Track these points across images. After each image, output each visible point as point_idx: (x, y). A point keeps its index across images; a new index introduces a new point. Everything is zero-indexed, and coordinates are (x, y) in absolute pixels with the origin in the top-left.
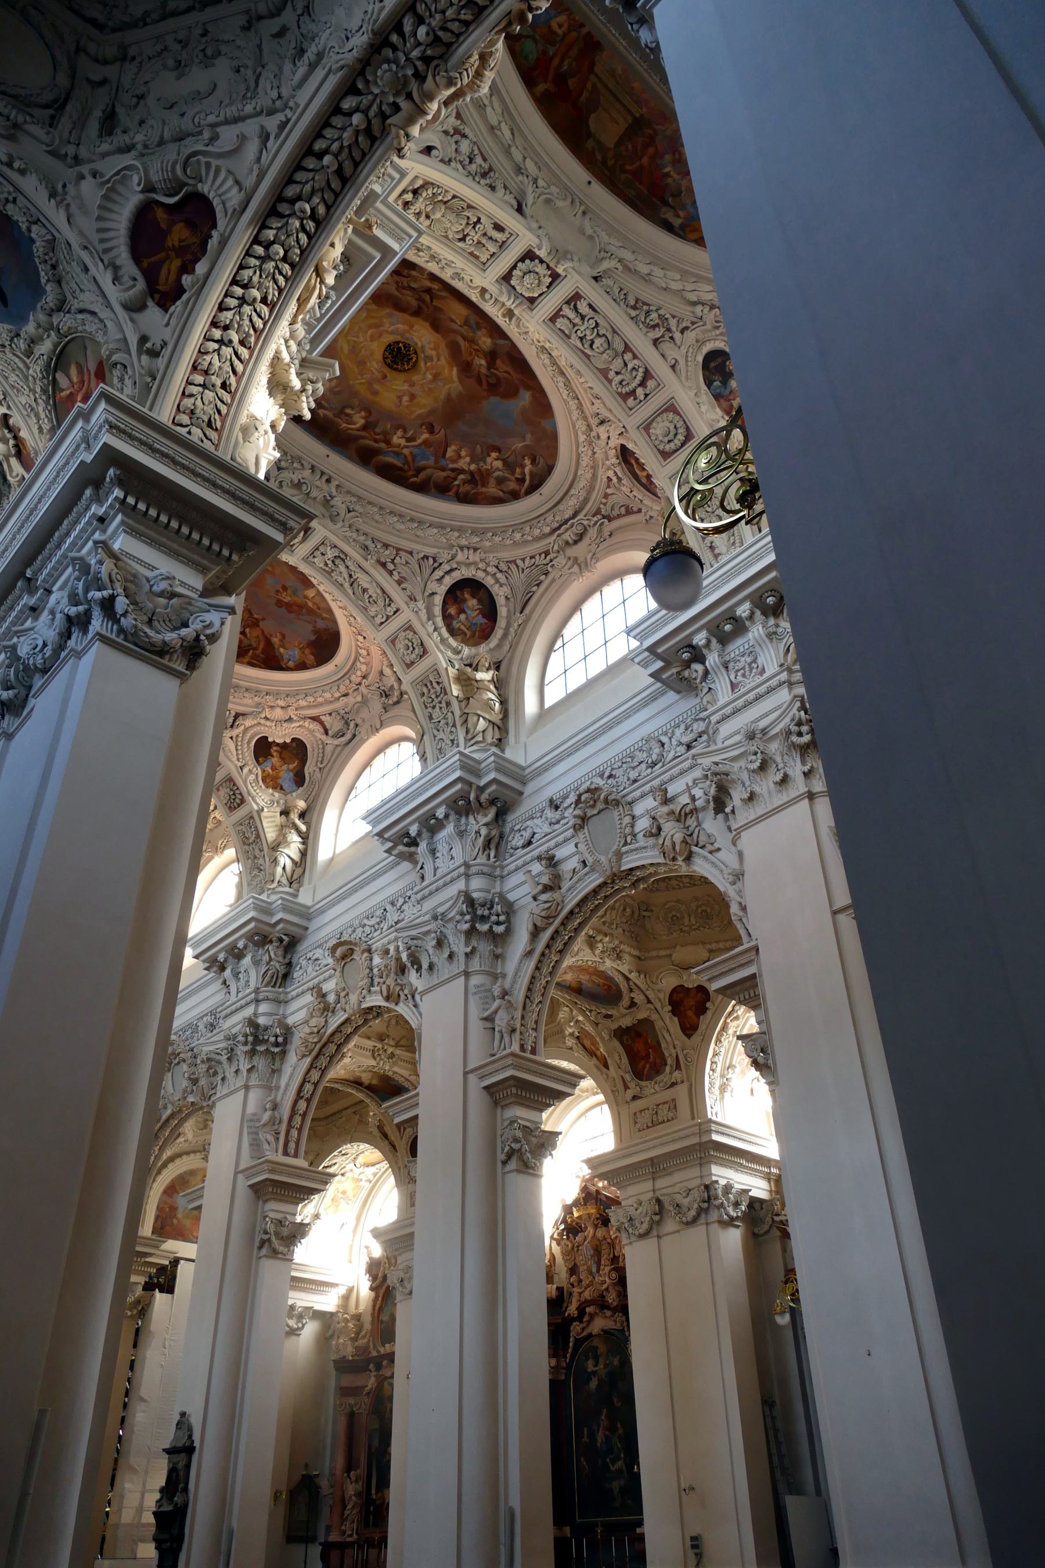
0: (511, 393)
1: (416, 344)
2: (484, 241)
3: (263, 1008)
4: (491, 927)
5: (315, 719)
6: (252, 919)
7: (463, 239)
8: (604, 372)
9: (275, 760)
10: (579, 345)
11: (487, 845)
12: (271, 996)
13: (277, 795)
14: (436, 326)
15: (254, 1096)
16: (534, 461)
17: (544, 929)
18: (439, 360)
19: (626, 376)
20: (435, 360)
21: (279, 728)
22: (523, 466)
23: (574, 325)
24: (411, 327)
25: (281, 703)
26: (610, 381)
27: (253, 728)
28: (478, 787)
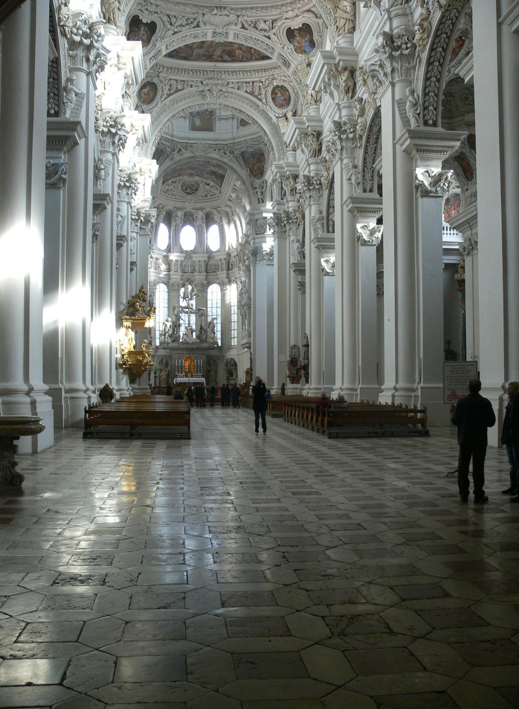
3: (312, 167)
4: (347, 135)
5: (309, 11)
6: (296, 129)
9: (298, 38)
11: (347, 92)
12: (313, 161)
13: (303, 56)
15: (313, 208)
17: (364, 135)
21: (294, 22)
25: (290, 8)
27: (282, 26)
28: (335, 64)
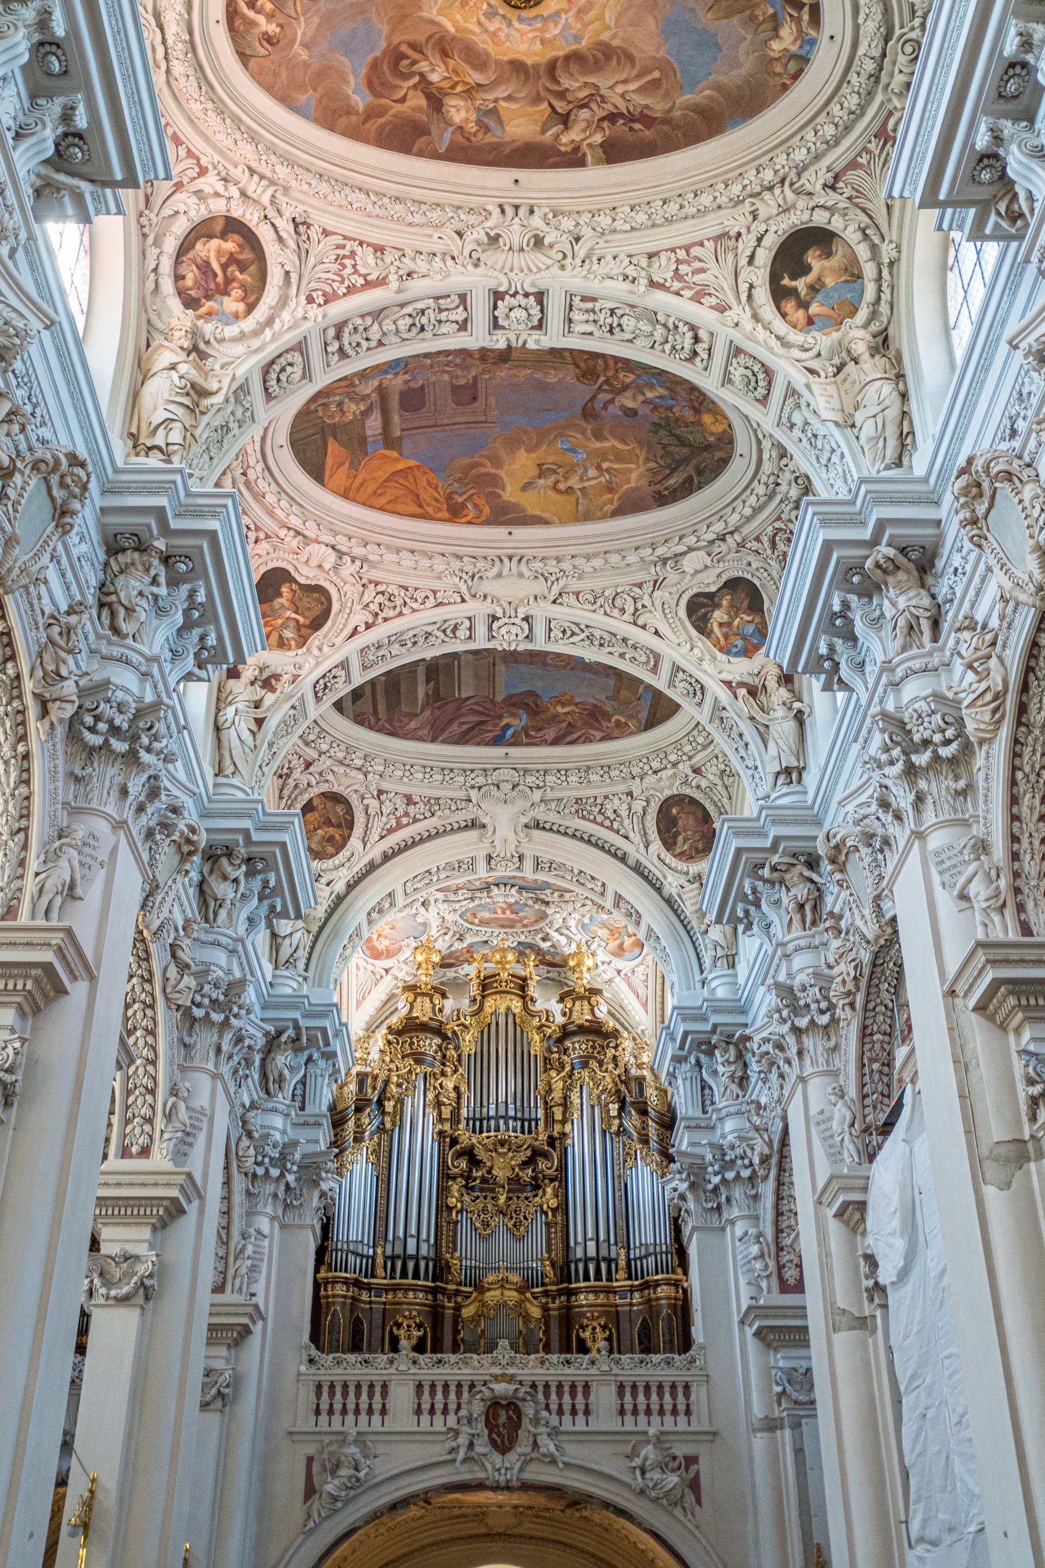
0: (375, 83)
1: (520, 20)
2: (592, 317)
7: (612, 312)
8: (377, 314)
10: (420, 305)
14: (517, 67)
16: (268, 39)
18: (479, 23)
19: (357, 338)
20: (483, 19)
22: (270, 17)
23: (441, 310)
24: (543, 41)
26: (363, 316)
